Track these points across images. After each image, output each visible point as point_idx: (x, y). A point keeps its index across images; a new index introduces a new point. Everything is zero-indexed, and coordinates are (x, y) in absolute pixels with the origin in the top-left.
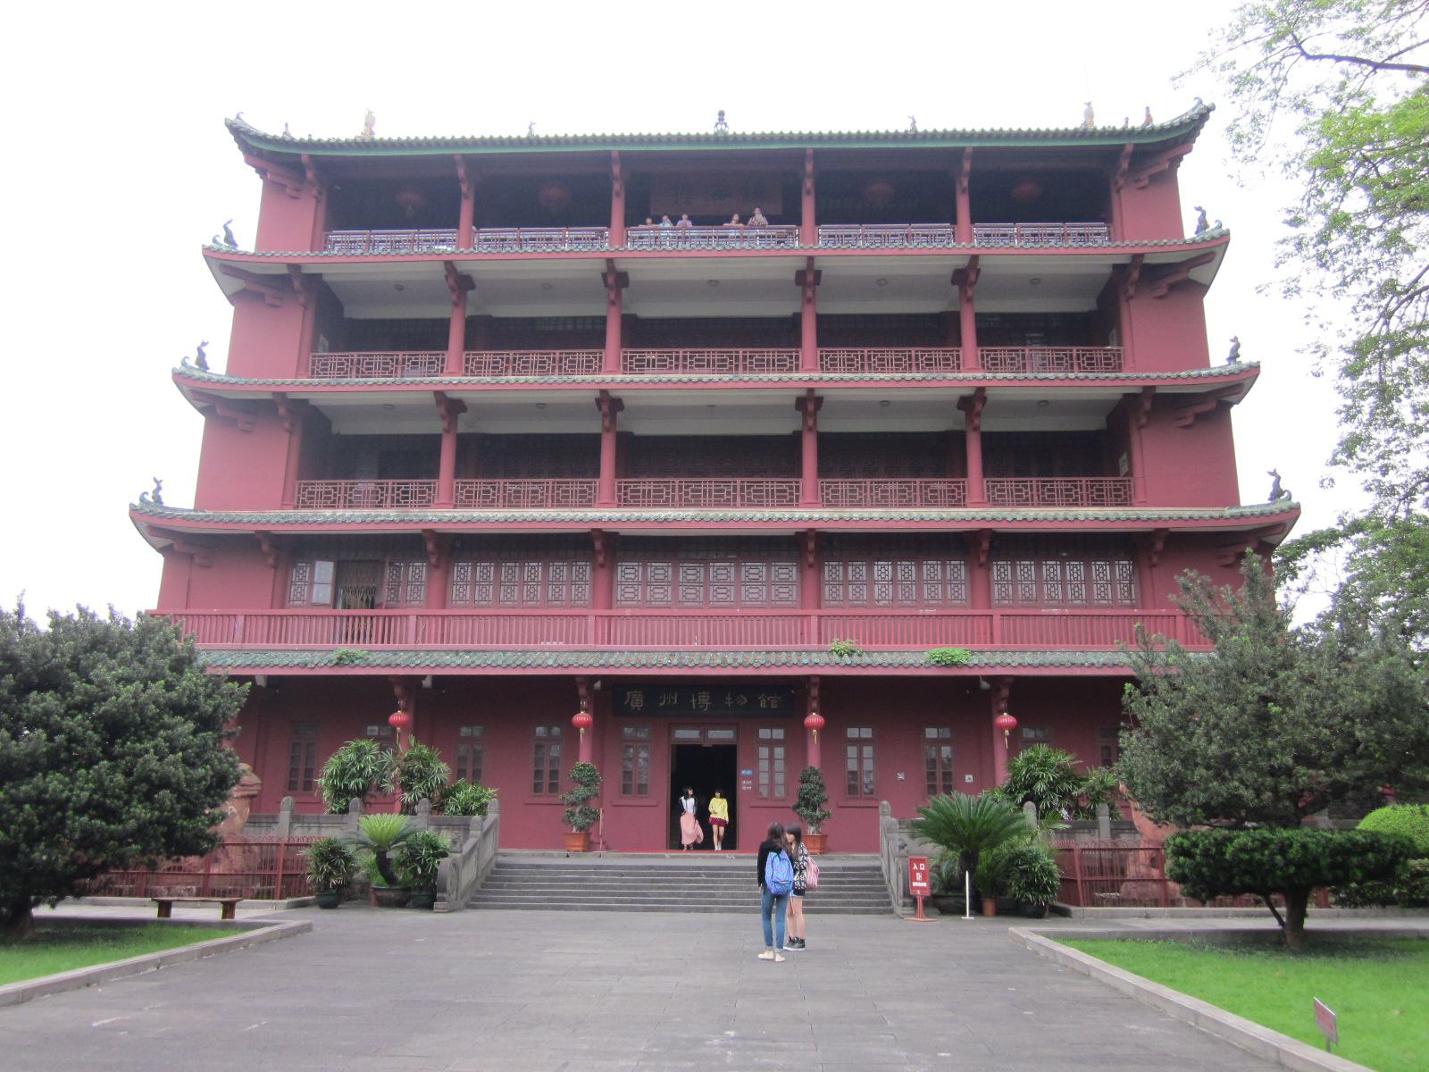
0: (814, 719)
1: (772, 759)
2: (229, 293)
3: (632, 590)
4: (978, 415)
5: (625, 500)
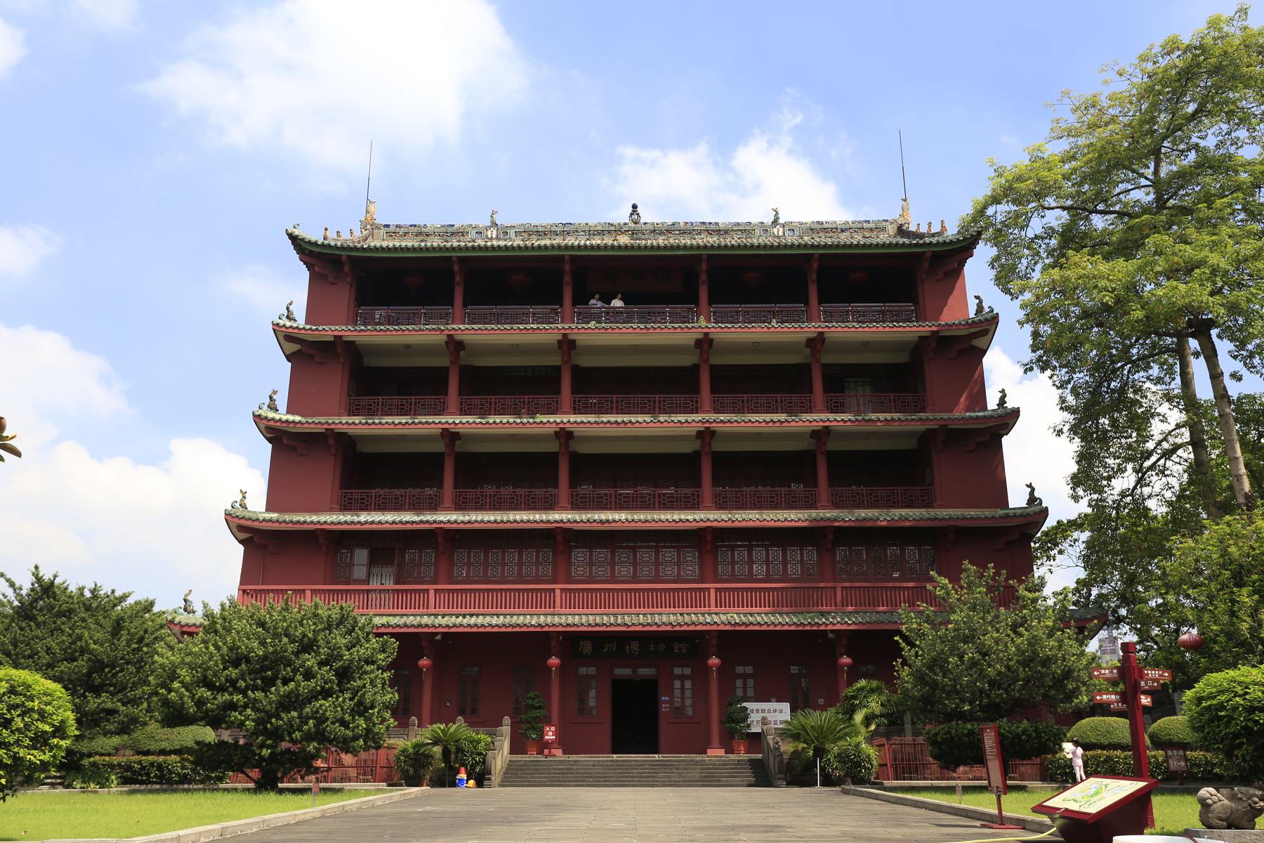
0: (714, 661)
1: (683, 689)
2: (287, 353)
3: (582, 569)
4: (825, 444)
5: (577, 504)
